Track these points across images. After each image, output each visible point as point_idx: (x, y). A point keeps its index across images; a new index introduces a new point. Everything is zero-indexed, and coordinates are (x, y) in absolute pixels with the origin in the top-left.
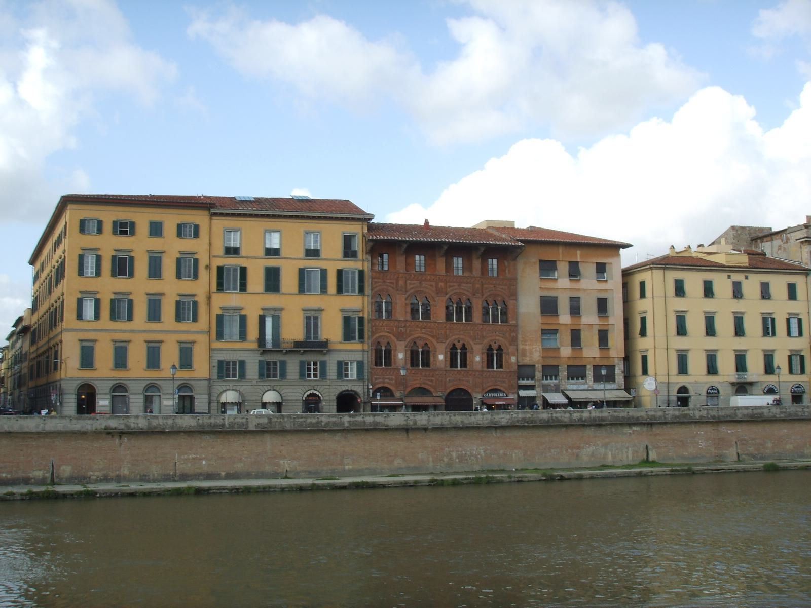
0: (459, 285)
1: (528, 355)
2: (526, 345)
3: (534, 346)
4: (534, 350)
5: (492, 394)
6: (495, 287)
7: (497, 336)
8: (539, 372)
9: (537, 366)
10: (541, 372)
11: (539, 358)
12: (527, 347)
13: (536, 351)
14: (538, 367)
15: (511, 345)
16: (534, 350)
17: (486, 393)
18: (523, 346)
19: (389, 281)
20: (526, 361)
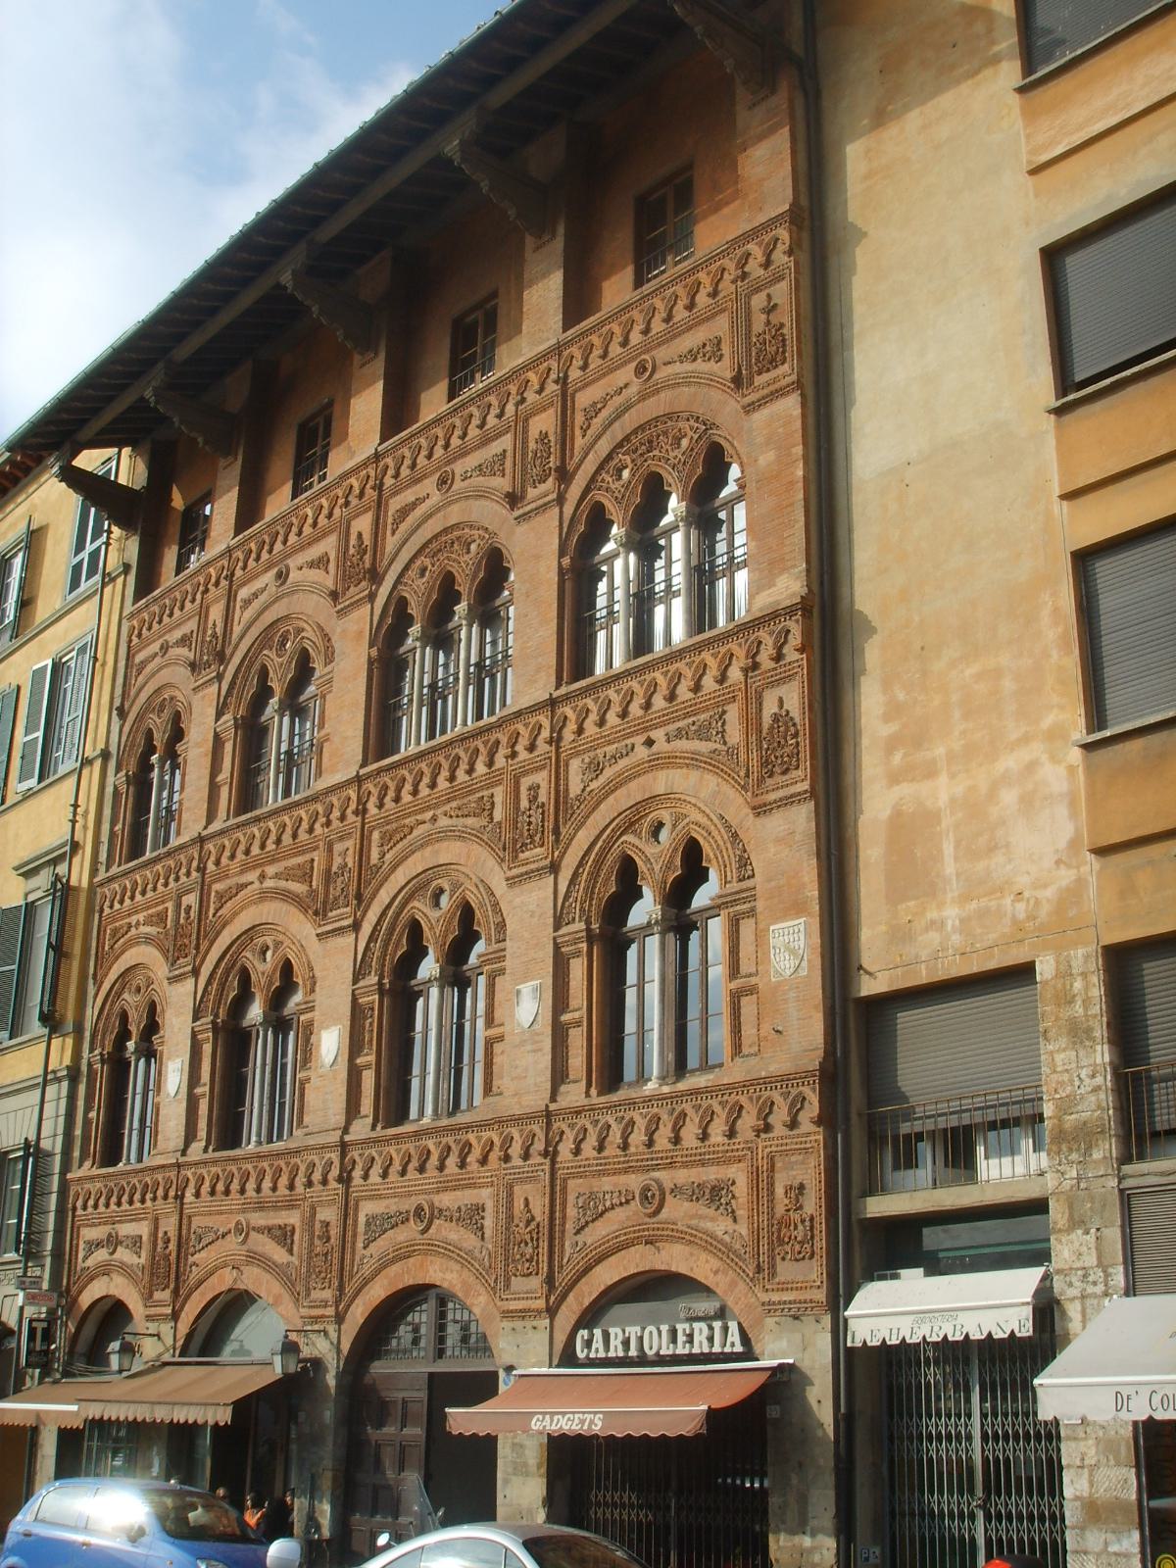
0: (444, 482)
1: (950, 868)
2: (931, 772)
3: (1010, 762)
4: (1009, 797)
5: (633, 1331)
6: (640, 369)
7: (657, 763)
8: (1078, 1033)
9: (1045, 969)
10: (1100, 1031)
11: (1066, 876)
12: (942, 791)
13: (1028, 803)
14: (1065, 974)
15: (761, 810)
16: (1009, 797)
17: (590, 1317)
18: (905, 790)
19: (177, 634)
20: (934, 937)
